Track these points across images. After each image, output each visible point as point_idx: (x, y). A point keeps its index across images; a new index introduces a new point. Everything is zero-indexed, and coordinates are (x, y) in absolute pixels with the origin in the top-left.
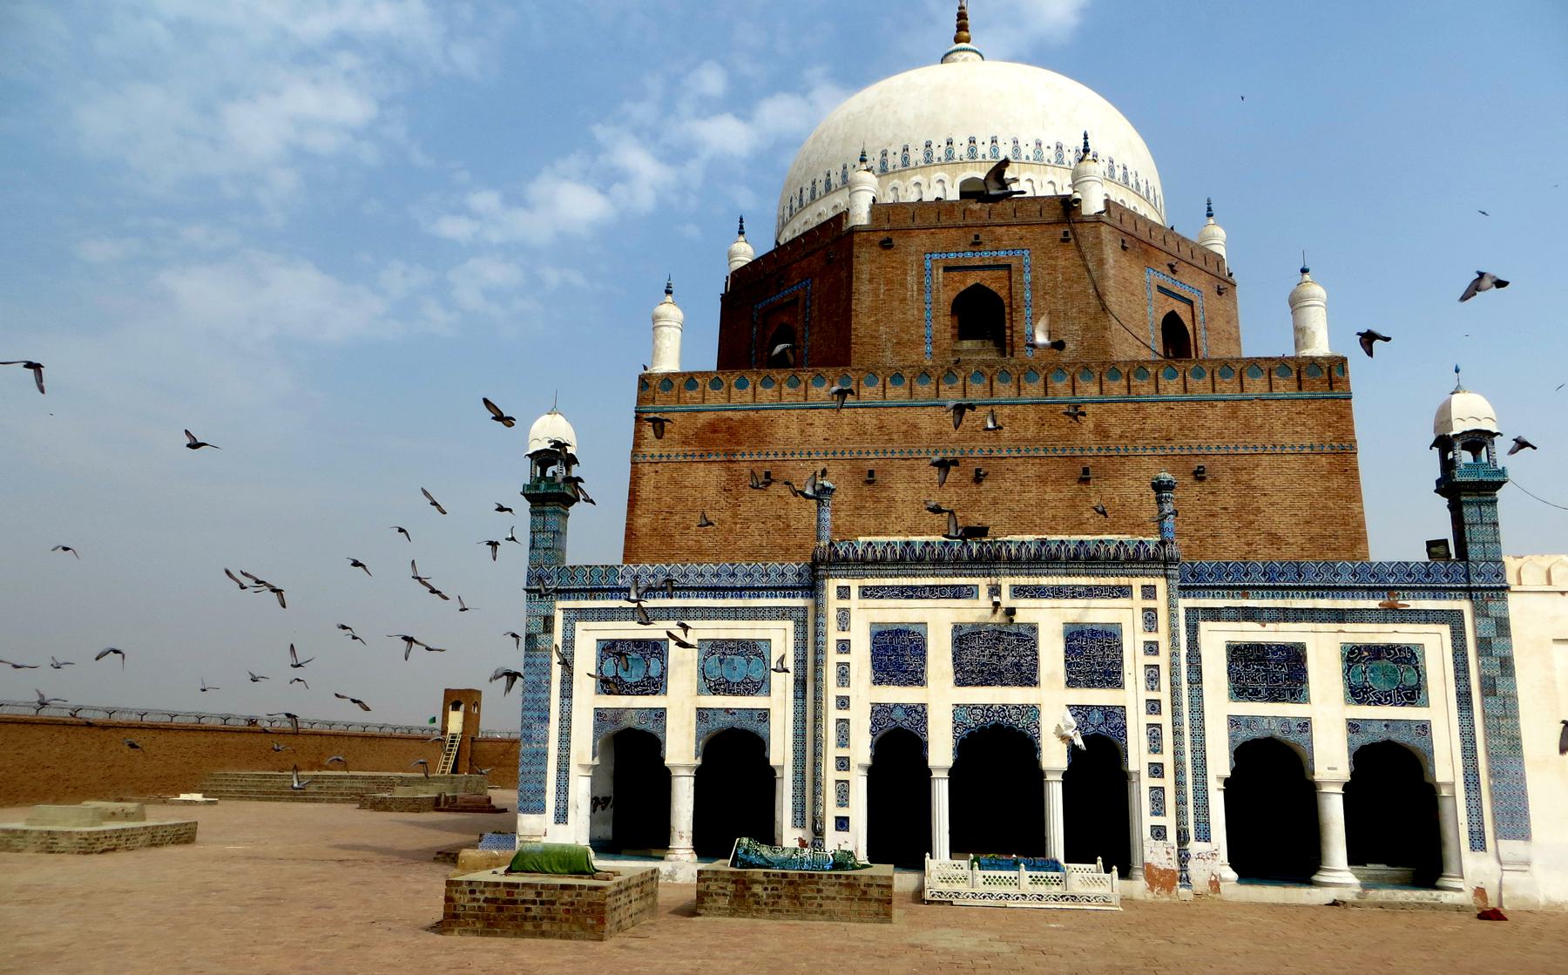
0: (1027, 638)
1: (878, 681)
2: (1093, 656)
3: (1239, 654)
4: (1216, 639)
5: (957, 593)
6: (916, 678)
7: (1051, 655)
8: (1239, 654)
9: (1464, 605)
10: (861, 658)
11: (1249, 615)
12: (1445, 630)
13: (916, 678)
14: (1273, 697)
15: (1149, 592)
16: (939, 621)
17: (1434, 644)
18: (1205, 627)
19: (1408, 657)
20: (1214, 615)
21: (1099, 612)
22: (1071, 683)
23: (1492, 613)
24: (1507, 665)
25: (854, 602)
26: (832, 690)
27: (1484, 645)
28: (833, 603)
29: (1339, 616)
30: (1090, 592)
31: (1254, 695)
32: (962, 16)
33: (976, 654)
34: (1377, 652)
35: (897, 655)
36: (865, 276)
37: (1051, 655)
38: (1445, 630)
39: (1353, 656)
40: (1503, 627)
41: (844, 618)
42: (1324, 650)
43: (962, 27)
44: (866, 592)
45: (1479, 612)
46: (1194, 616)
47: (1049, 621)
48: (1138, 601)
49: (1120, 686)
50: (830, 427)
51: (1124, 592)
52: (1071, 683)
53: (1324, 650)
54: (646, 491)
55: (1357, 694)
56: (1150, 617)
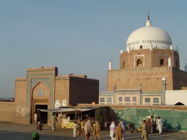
0: (129, 98)
1: (119, 101)
2: (134, 99)
3: (146, 99)
4: (144, 98)
5: (125, 94)
6: (122, 101)
7: (131, 99)
8: (146, 99)
9: (162, 95)
10: (118, 100)
11: (146, 96)
12: (161, 97)
13: (122, 101)
14: (148, 102)
15: (138, 94)
16: (123, 97)
17: (160, 98)
18: (143, 96)
19: (158, 99)
20: (144, 96)
21: (135, 96)
22: (133, 101)
23: (164, 95)
24: (165, 99)
25: (117, 95)
26: (116, 102)
27: (163, 98)
28: (116, 95)
29: (153, 96)
30: (134, 94)
31: (147, 102)
32: (149, 17)
33: (126, 99)
34: (155, 98)
35: (120, 99)
36: (129, 58)
37: (131, 99)
38: (161, 97)
39: (154, 99)
40: (165, 96)
41: (117, 96)
42: (152, 98)
43: (149, 18)
44: (118, 94)
45: (163, 95)
46: (142, 96)
47: (131, 97)
48: (138, 95)
49: (136, 101)
50: (125, 75)
51: (136, 94)
52: (133, 101)
53: (152, 98)
54: (109, 81)
55: (154, 102)
56: (138, 96)
